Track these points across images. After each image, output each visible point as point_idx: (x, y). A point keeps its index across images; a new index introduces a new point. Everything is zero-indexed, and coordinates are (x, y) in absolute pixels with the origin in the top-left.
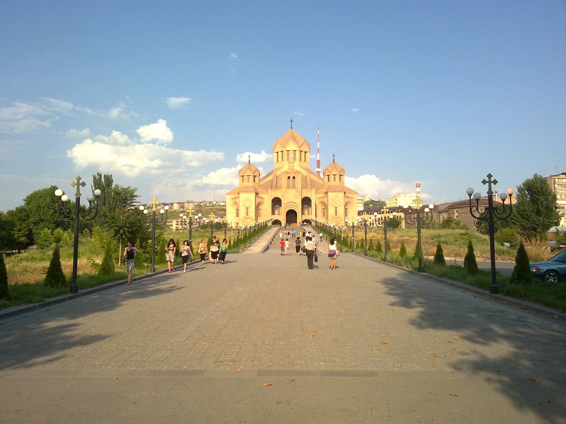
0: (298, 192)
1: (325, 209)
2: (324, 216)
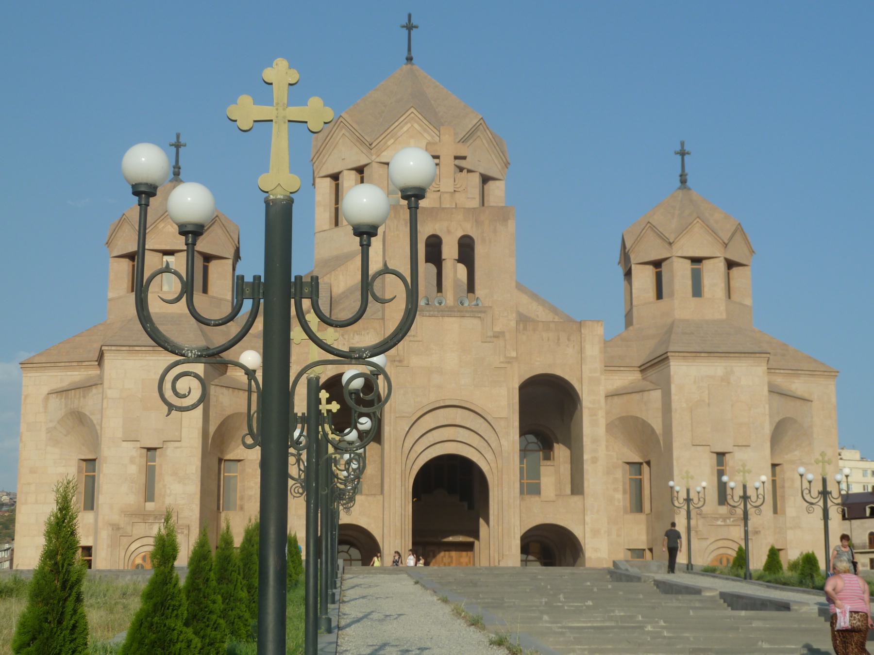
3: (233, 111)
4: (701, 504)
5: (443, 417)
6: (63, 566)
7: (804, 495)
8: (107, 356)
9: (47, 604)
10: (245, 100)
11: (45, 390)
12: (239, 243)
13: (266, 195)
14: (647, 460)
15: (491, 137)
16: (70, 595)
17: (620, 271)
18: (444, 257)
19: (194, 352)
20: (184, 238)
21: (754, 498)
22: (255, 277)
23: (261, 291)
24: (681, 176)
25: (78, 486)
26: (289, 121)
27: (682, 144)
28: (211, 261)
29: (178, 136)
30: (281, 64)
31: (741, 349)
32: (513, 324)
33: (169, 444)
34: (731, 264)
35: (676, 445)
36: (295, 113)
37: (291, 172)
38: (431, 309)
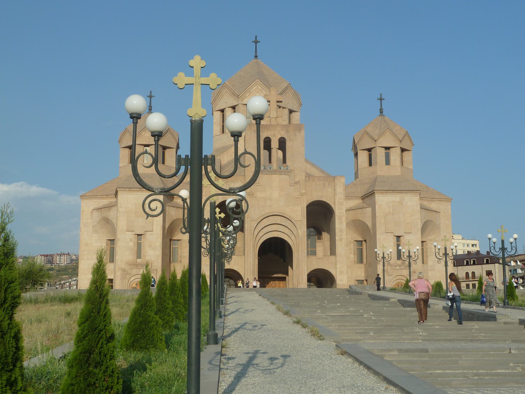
0: (297, 183)
1: (364, 243)
2: (361, 261)
3: (176, 80)
4: (389, 259)
5: (272, 220)
6: (100, 288)
7: (436, 255)
8: (119, 193)
9: (93, 305)
10: (181, 75)
11: (92, 208)
12: (179, 141)
13: (191, 118)
14: (364, 239)
15: (293, 92)
16: (103, 301)
17: (352, 154)
18: (272, 147)
19: (158, 190)
20: (153, 138)
21: (413, 257)
22: (186, 155)
23: (189, 162)
24: (380, 110)
25: (106, 252)
26: (201, 84)
27: (381, 95)
28: (166, 149)
29: (151, 92)
30: (197, 58)
31: (407, 189)
32: (304, 177)
33: (147, 232)
34: (403, 150)
35: (377, 232)
36: (204, 80)
37: (202, 108)
38: (266, 171)
